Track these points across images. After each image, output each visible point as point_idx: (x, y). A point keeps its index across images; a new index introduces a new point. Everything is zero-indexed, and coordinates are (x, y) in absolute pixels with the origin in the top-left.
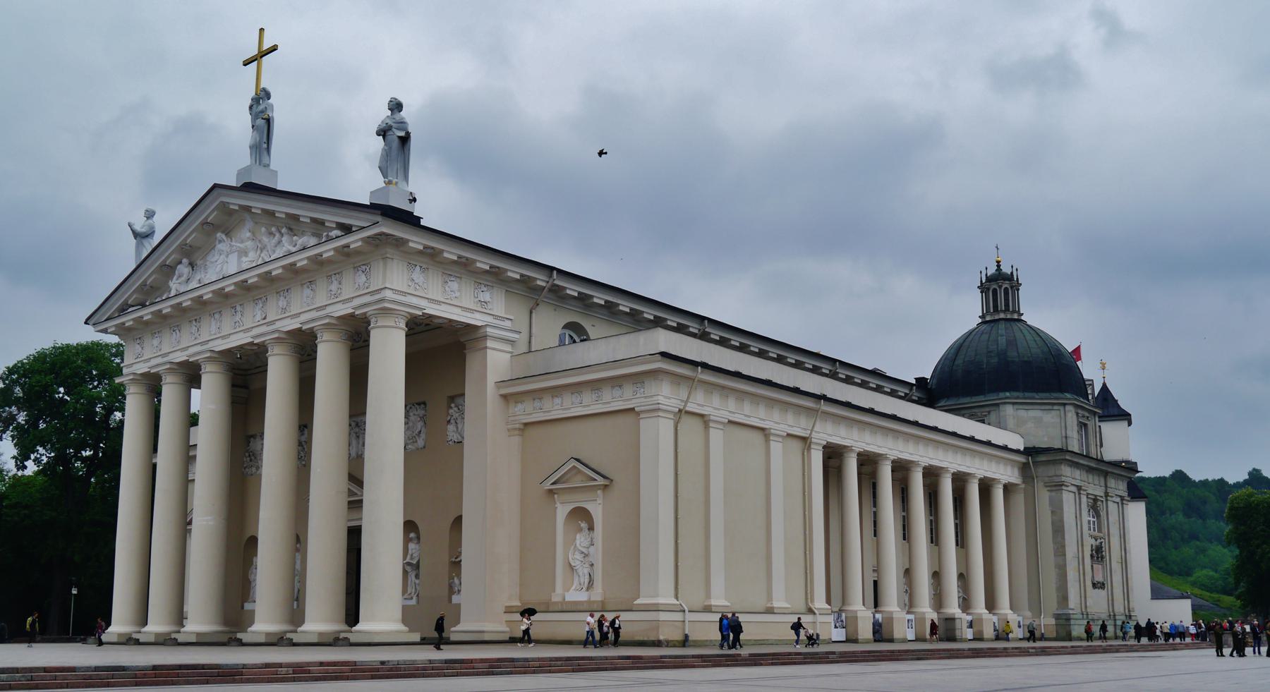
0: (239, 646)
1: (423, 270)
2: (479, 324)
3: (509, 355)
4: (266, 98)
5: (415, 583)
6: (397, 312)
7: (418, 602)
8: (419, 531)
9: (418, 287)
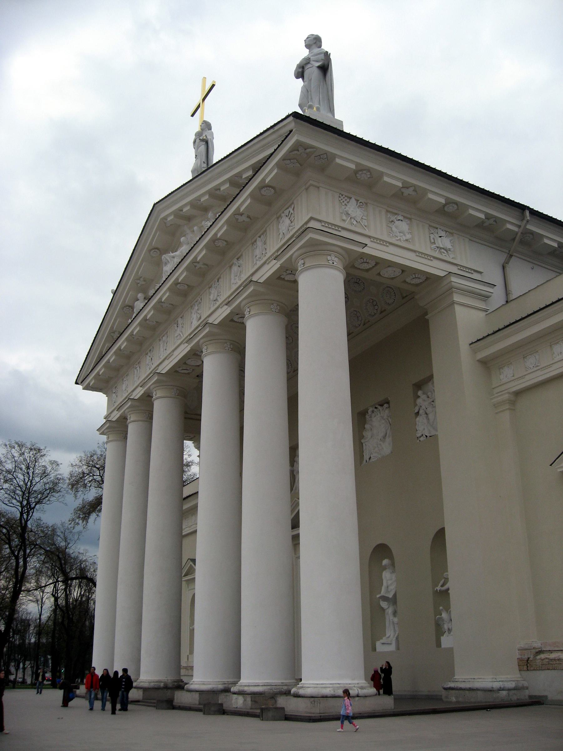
0: (169, 708)
1: (361, 205)
2: (442, 274)
3: (484, 314)
4: (207, 129)
5: (393, 623)
6: (329, 247)
7: (398, 648)
8: (392, 554)
9: (355, 223)
